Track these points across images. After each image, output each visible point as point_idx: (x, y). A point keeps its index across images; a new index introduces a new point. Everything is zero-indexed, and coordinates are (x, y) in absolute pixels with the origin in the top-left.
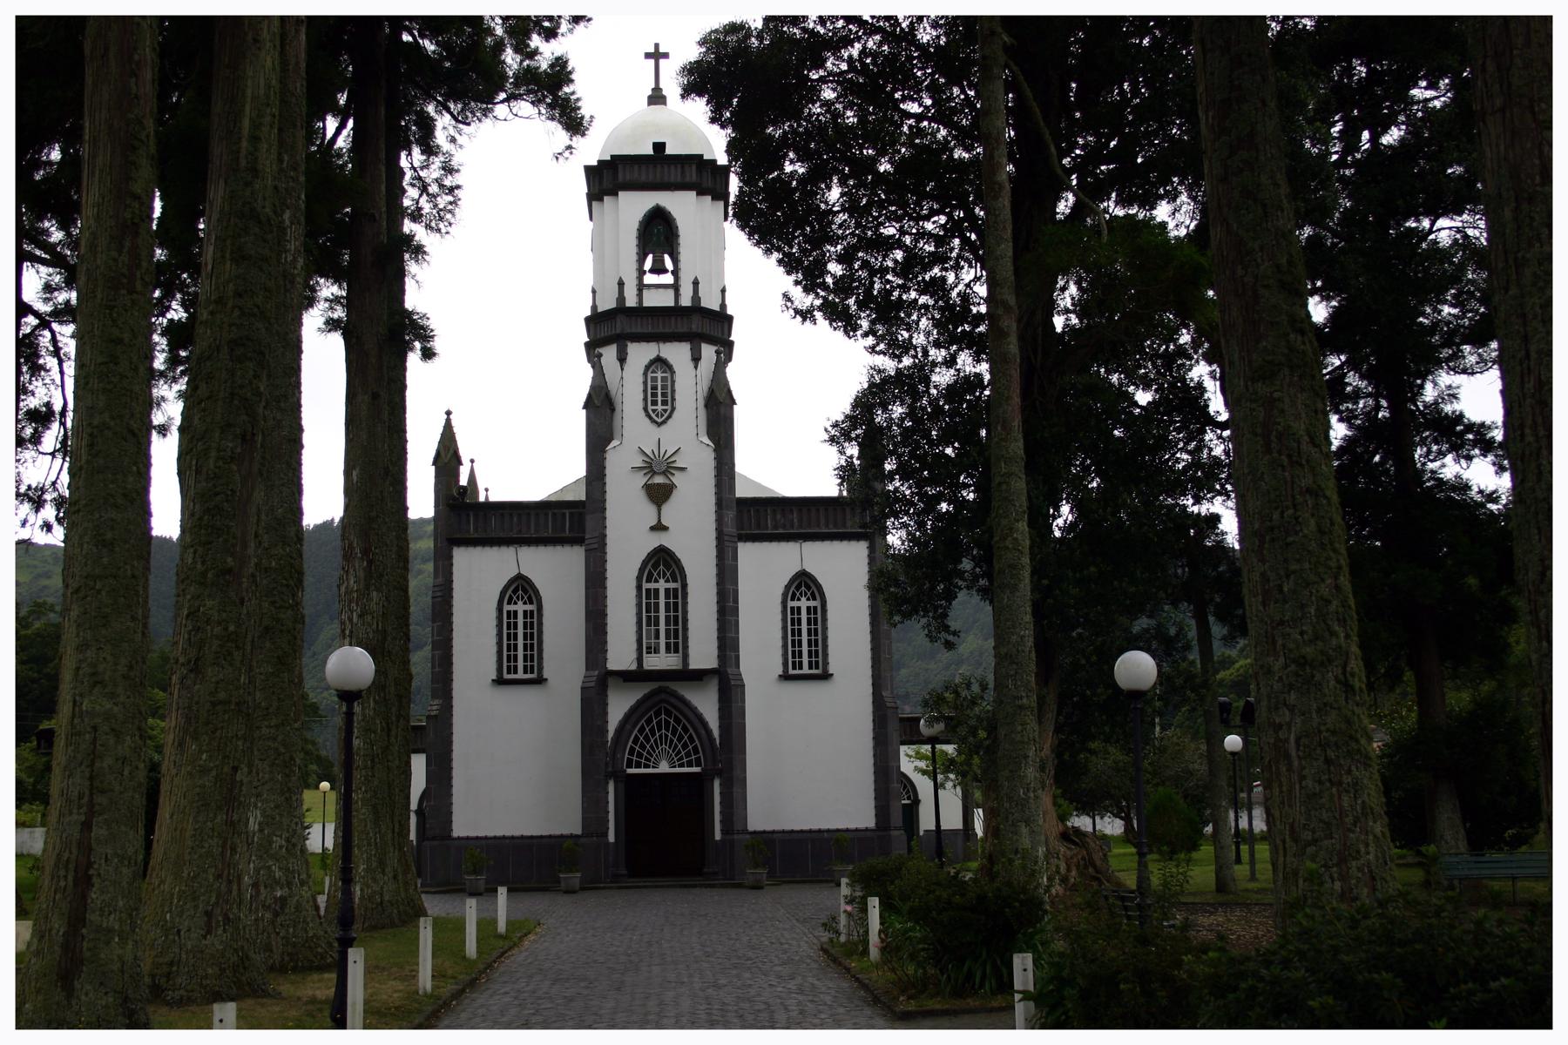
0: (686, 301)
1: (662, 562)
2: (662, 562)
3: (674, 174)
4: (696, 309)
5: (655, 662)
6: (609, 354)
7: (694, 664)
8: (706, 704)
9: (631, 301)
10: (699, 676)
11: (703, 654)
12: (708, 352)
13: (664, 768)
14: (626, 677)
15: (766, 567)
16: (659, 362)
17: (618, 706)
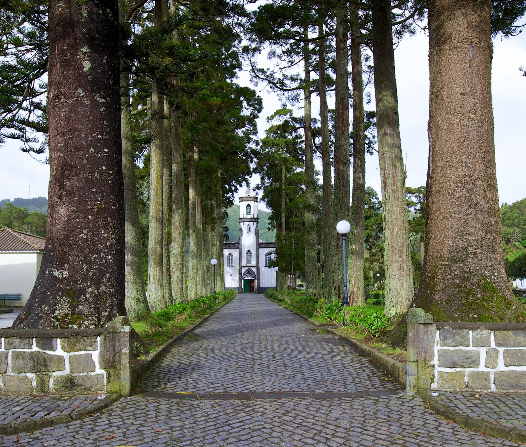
0: (252, 217)
1: (249, 251)
2: (249, 251)
3: (251, 199)
4: (254, 218)
5: (248, 265)
6: (242, 223)
7: (253, 265)
8: (254, 270)
9: (245, 217)
10: (254, 267)
11: (254, 263)
12: (255, 223)
13: (249, 278)
14: (244, 267)
15: (264, 252)
16: (249, 225)
17: (244, 270)
